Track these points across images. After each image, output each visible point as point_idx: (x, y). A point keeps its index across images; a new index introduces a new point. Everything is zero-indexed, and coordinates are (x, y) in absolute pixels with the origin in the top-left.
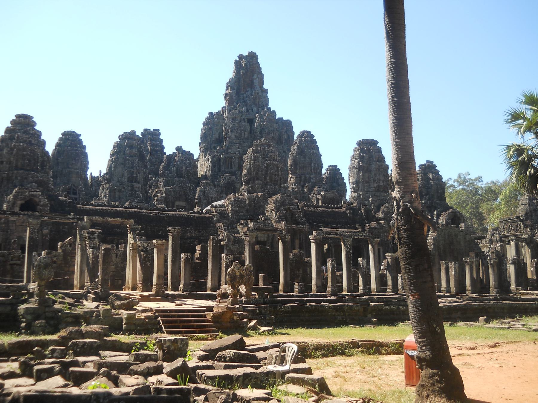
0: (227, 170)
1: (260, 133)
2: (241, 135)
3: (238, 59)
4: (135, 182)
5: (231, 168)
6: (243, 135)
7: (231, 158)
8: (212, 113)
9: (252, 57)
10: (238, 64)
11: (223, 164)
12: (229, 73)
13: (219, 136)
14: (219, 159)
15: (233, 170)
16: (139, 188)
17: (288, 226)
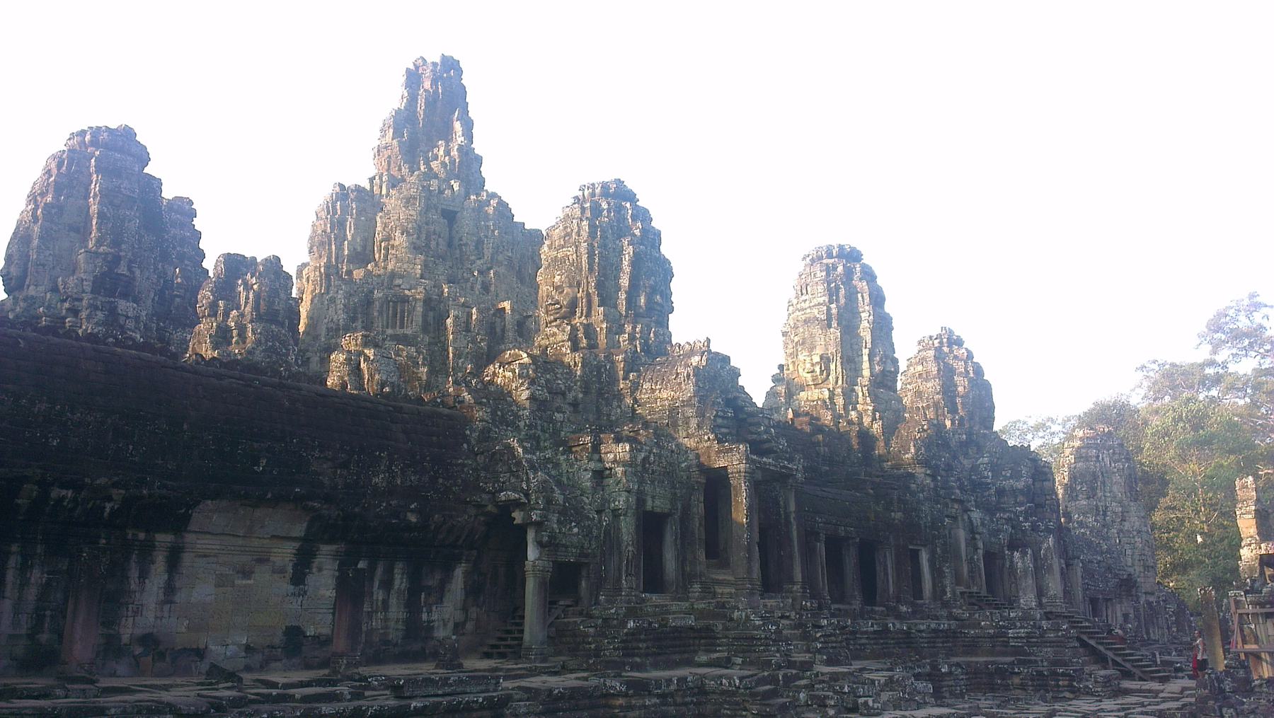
0: (389, 331)
1: (477, 248)
2: (428, 246)
3: (412, 67)
4: (125, 296)
5: (402, 327)
6: (433, 244)
7: (405, 300)
8: (342, 186)
9: (450, 66)
10: (413, 78)
11: (381, 313)
12: (393, 97)
13: (364, 247)
14: (368, 302)
15: (409, 332)
16: (137, 319)
17: (753, 461)
